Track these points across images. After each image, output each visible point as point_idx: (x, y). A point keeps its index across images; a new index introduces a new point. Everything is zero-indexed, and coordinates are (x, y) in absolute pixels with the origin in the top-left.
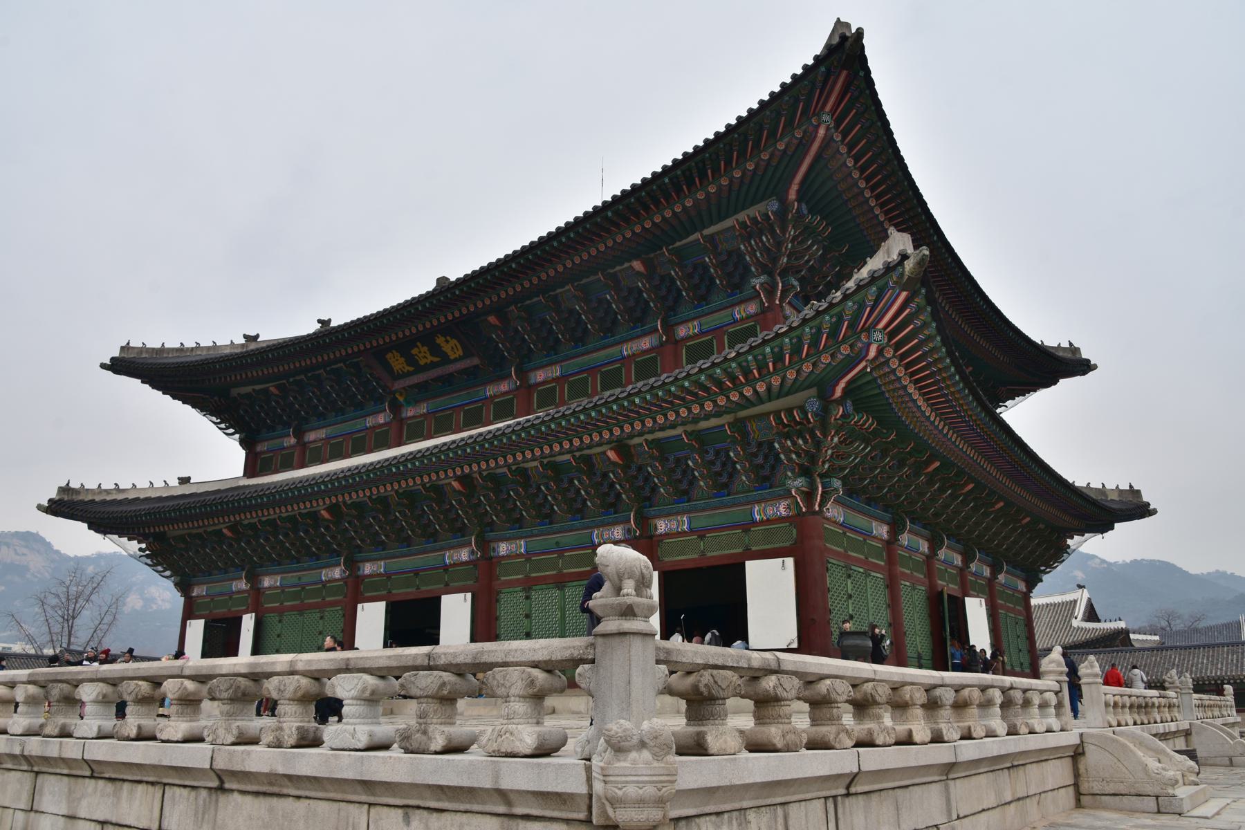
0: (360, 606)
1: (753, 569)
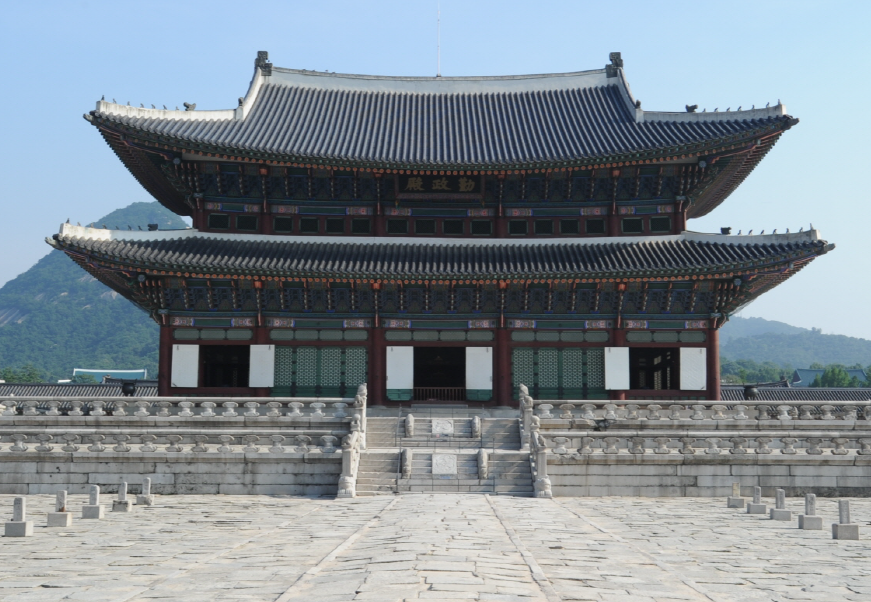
0: (389, 348)
1: (685, 352)
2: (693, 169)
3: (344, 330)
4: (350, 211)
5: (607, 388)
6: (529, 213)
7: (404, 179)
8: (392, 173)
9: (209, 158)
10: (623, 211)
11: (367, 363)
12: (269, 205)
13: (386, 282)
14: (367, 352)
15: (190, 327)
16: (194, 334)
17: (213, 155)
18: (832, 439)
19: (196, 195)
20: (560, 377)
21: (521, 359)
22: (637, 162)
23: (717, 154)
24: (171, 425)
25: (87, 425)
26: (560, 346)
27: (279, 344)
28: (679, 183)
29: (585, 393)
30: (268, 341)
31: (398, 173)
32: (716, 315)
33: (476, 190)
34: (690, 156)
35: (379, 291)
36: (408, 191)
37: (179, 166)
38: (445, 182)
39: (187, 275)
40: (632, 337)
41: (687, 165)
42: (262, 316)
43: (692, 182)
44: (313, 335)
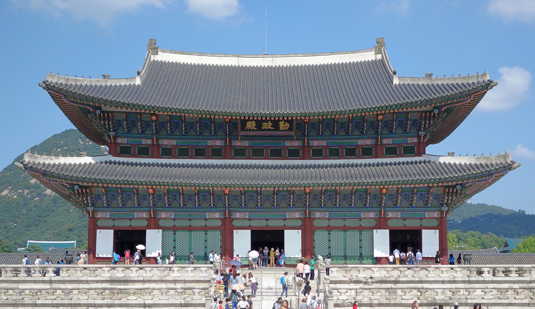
0: (235, 231)
2: (430, 115)
3: (206, 220)
4: (210, 143)
5: (375, 256)
6: (324, 143)
7: (244, 122)
8: (236, 119)
9: (119, 109)
10: (385, 141)
11: (221, 240)
12: (157, 139)
13: (233, 189)
14: (221, 234)
15: (107, 218)
16: (111, 223)
17: (122, 108)
18: (515, 290)
19: (111, 133)
20: (345, 249)
21: (320, 237)
22: (394, 110)
23: (445, 105)
24: (97, 282)
25: (44, 282)
26: (345, 229)
27: (164, 229)
28: (421, 123)
29: (361, 258)
30: (157, 227)
31: (240, 119)
32: (445, 208)
33: (290, 129)
34: (428, 106)
35: (229, 195)
36: (247, 130)
37: (100, 115)
38: (270, 124)
39: (105, 185)
40: (391, 223)
41: (426, 112)
42: (153, 211)
43: (430, 123)
44: (187, 223)
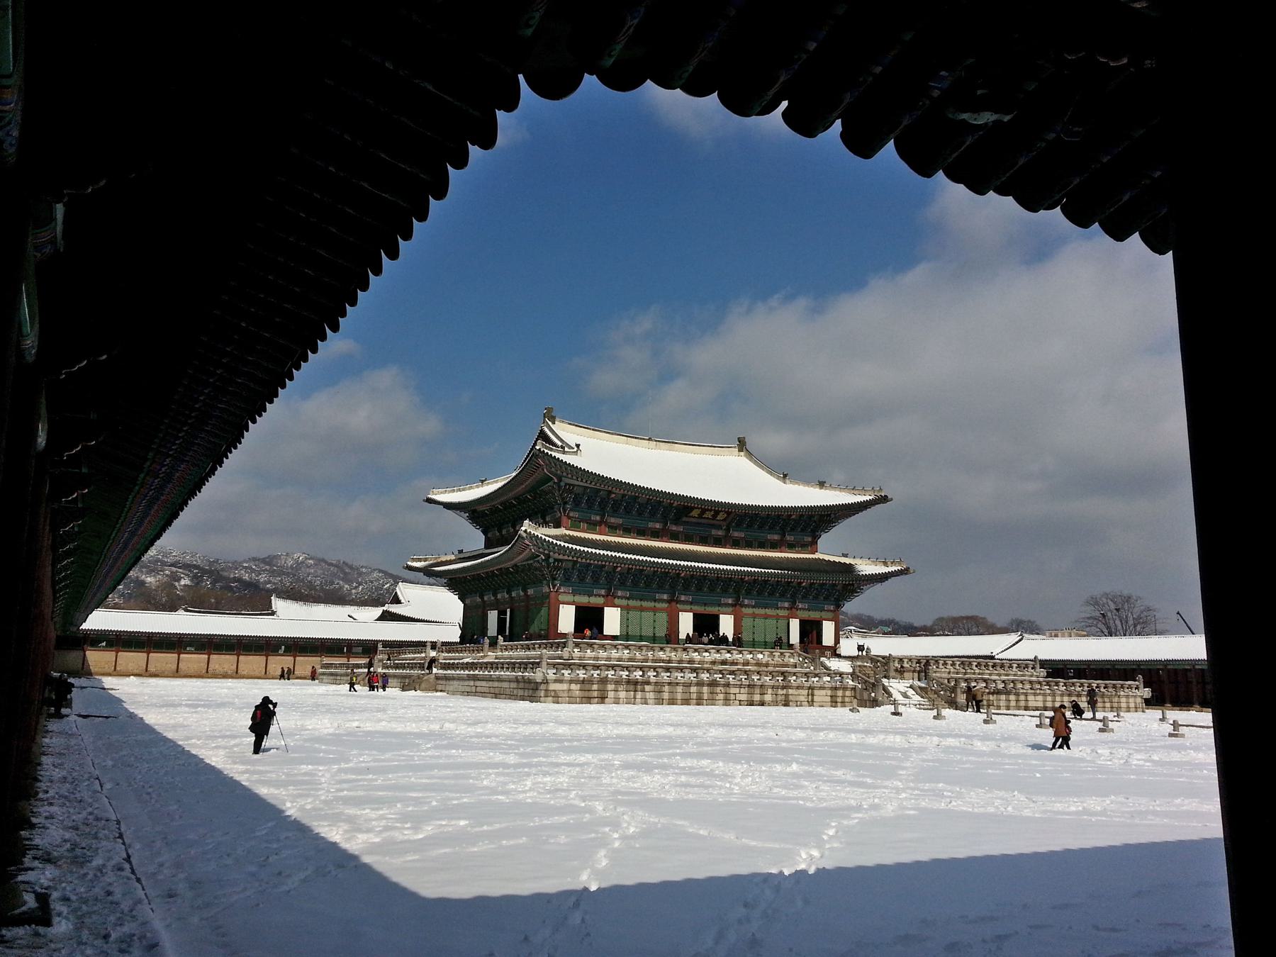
4: (651, 525)
